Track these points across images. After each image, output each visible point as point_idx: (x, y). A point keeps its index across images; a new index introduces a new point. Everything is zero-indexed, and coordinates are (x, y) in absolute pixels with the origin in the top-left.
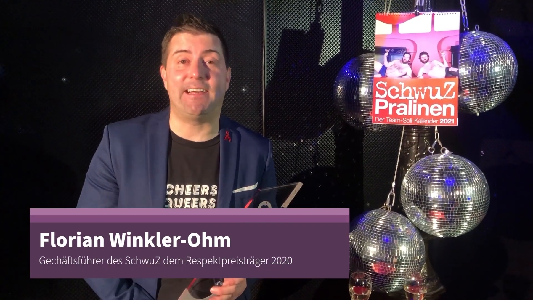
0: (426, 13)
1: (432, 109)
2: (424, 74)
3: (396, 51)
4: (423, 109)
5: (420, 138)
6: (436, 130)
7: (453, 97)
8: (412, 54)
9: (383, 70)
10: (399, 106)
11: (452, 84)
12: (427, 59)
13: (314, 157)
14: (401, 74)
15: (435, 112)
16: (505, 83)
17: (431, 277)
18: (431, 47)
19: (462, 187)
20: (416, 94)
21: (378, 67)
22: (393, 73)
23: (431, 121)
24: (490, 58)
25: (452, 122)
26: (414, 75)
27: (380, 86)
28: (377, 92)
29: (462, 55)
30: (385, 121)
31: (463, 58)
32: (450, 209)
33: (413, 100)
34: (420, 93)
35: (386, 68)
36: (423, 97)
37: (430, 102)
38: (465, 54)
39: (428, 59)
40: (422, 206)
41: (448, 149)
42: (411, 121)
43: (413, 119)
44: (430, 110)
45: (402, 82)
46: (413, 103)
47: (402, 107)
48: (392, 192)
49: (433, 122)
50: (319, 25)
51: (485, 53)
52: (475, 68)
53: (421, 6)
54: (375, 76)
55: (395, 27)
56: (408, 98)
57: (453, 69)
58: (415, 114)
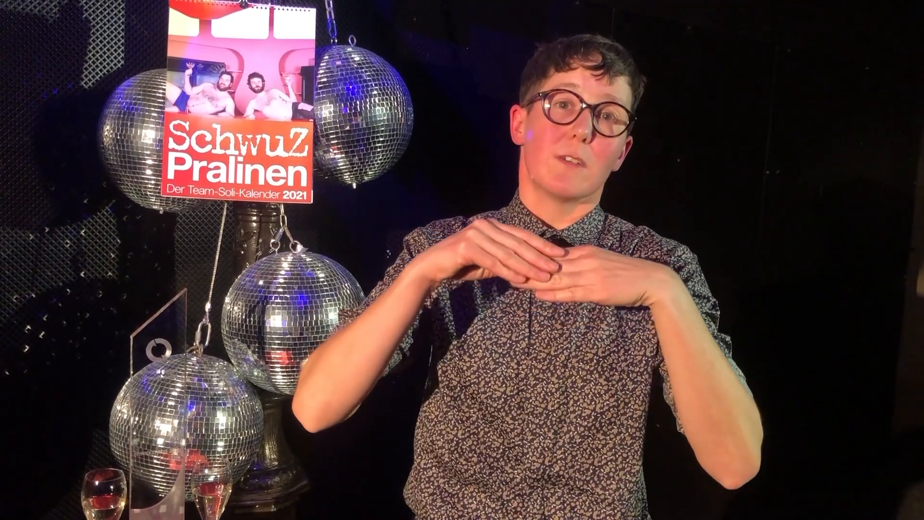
0: (260, 5)
1: (270, 174)
2: (256, 111)
3: (205, 68)
4: (255, 173)
5: (263, 225)
6: (282, 210)
7: (305, 154)
8: (234, 75)
9: (183, 100)
10: (212, 165)
11: (304, 132)
12: (261, 85)
13: (74, 261)
14: (215, 110)
15: (276, 179)
16: (390, 136)
17: (284, 466)
18: (268, 66)
19: (317, 307)
20: (241, 146)
21: (172, 92)
22: (200, 106)
23: (268, 195)
24: (363, 92)
25: (303, 196)
26: (239, 113)
27: (177, 127)
28: (171, 140)
30: (186, 191)
32: (295, 345)
33: (236, 156)
35: (188, 97)
36: (254, 151)
37: (267, 162)
39: (263, 86)
40: (251, 343)
41: (301, 244)
42: (232, 193)
44: (266, 175)
45: (217, 124)
46: (237, 162)
47: (217, 168)
48: (206, 320)
49: (271, 195)
50: (80, 10)
51: (356, 83)
52: (340, 105)
54: (167, 110)
55: (205, 25)
56: (228, 152)
57: (304, 106)
58: (240, 181)
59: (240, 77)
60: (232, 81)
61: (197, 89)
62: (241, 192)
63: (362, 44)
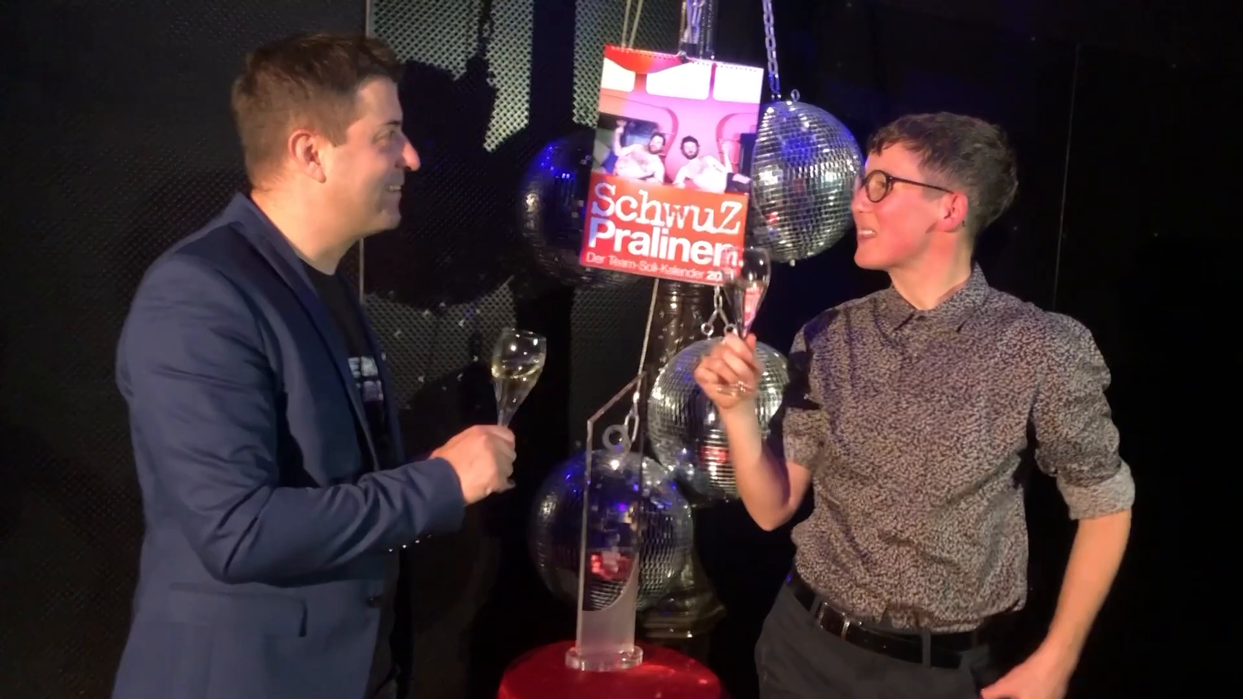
0: (701, 61)
2: (687, 179)
3: (639, 128)
4: (679, 249)
8: (667, 137)
10: (636, 235)
11: (737, 206)
12: (694, 150)
14: (643, 175)
15: (701, 257)
26: (668, 180)
29: (762, 147)
30: (607, 260)
31: (769, 151)
37: (693, 237)
38: (772, 145)
42: (654, 268)
43: (659, 266)
44: (691, 251)
46: (661, 235)
47: (640, 239)
55: (641, 78)
56: (653, 222)
58: (662, 256)
59: (673, 138)
60: (664, 144)
61: (627, 150)
62: (663, 268)
63: (806, 98)
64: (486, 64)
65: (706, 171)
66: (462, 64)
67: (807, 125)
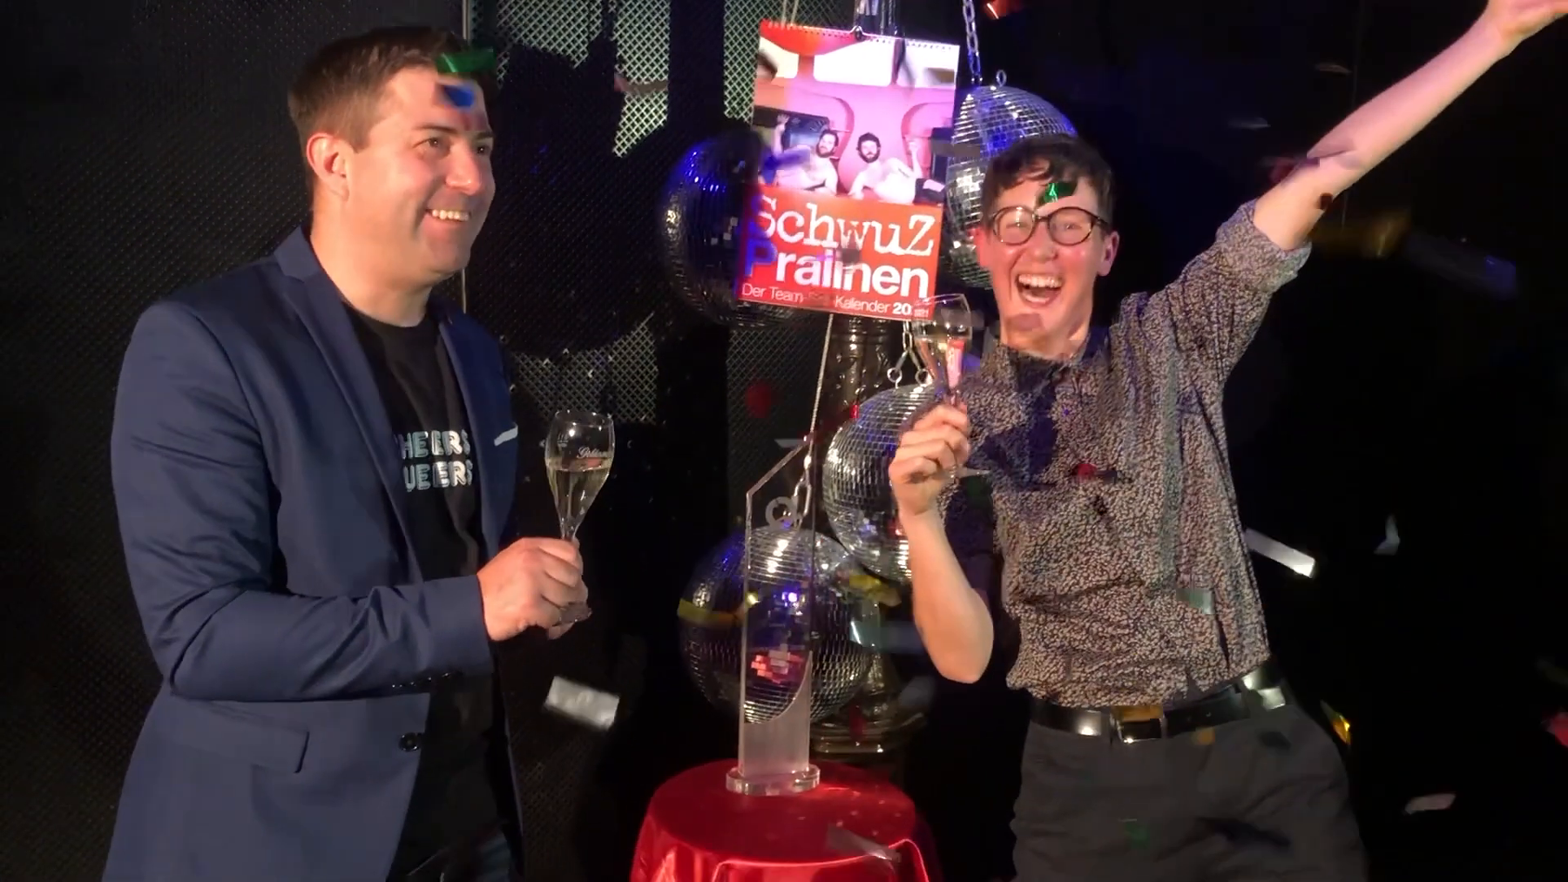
0: (882, 38)
1: (878, 277)
2: (865, 188)
3: (805, 123)
7: (928, 252)
10: (802, 261)
11: (928, 220)
12: (874, 151)
14: (811, 184)
15: (885, 285)
26: (842, 189)
30: (768, 293)
34: (852, 236)
47: (808, 265)
53: (871, 17)
55: (806, 62)
56: (825, 244)
57: (933, 185)
59: (846, 140)
64: (613, 46)
65: (890, 177)
66: (584, 48)
67: (1015, 115)
